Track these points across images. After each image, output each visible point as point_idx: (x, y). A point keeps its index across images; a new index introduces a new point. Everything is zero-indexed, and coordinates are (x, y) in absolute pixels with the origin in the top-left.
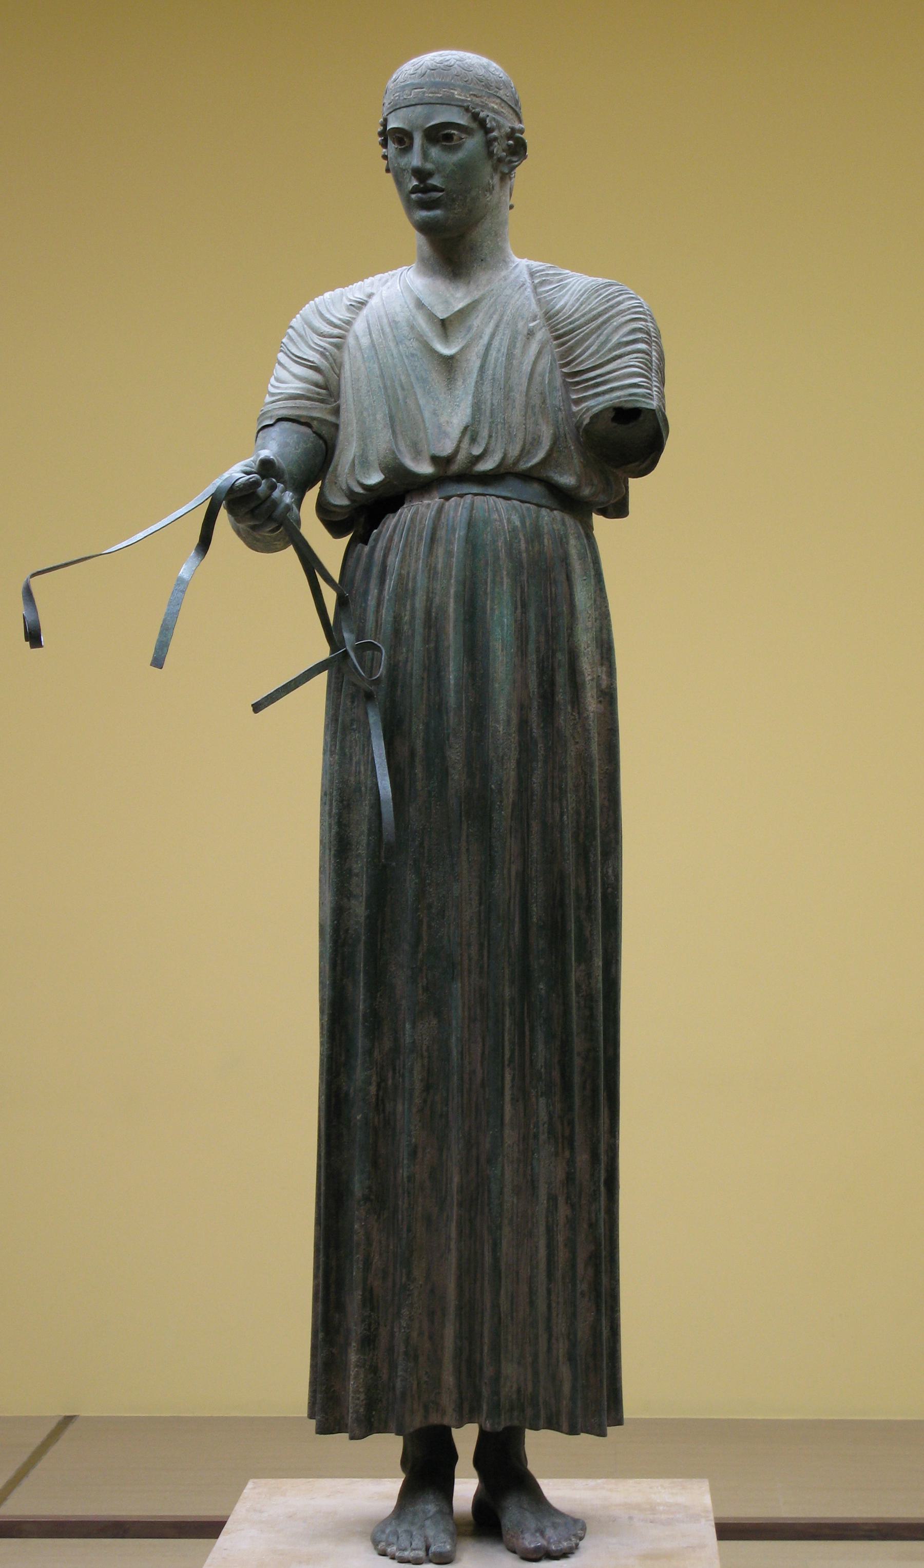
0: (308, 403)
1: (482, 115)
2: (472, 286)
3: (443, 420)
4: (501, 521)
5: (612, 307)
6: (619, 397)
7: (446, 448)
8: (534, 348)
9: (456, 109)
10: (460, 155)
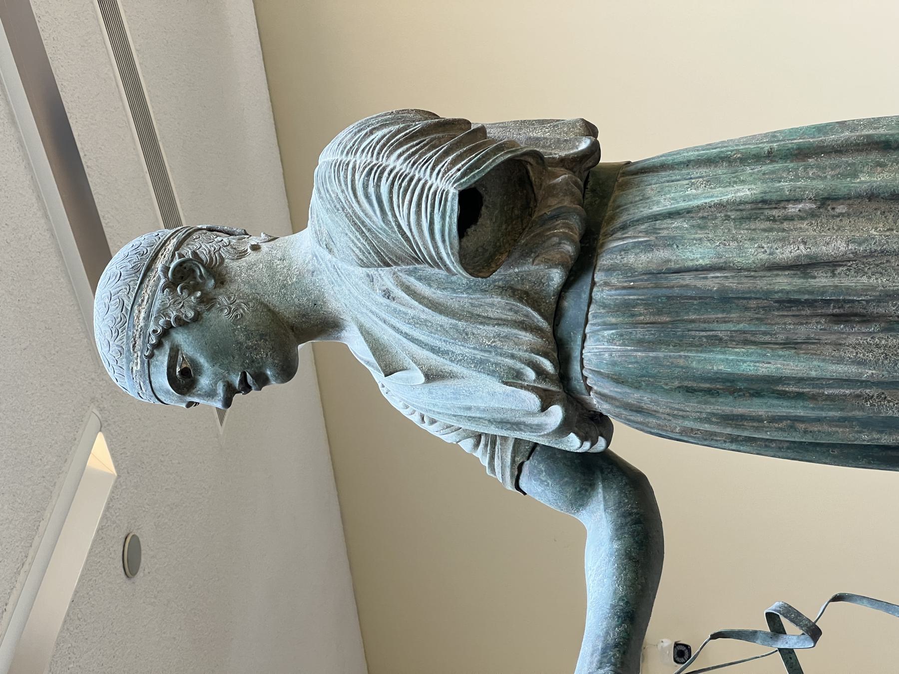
1: (154, 341)
2: (346, 323)
4: (611, 352)
6: (448, 254)
9: (153, 369)
10: (202, 360)
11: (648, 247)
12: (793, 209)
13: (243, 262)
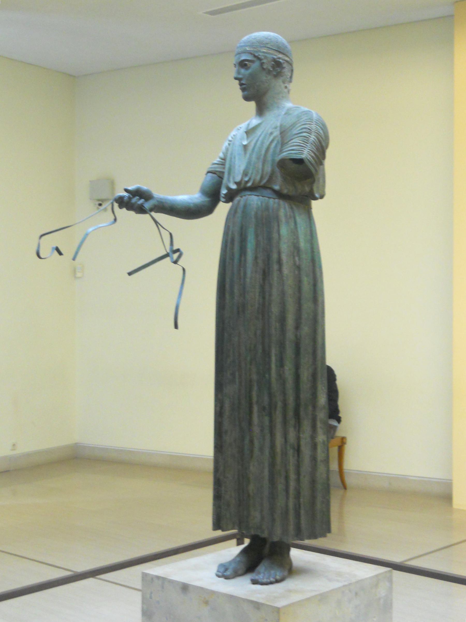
0: (216, 166)
1: (256, 54)
7: (238, 179)
8: (271, 138)
9: (247, 54)
11: (286, 216)
12: (297, 259)
13: (282, 84)
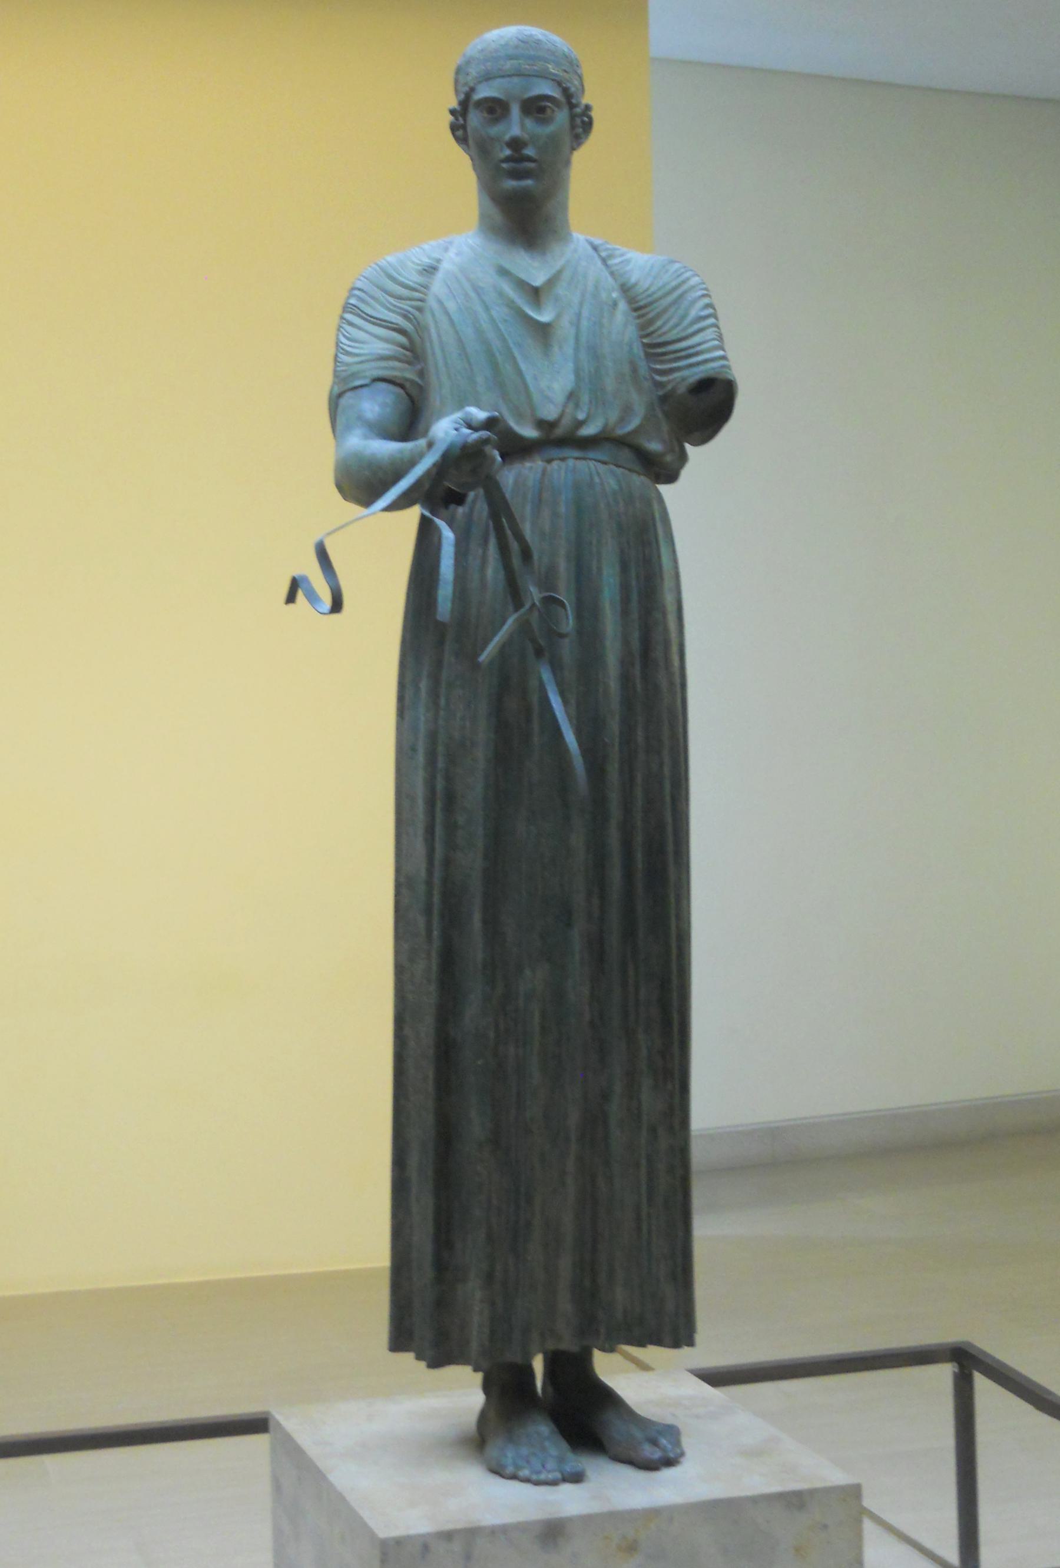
3: (543, 384)
4: (602, 484)
5: (684, 282)
7: (550, 413)
10: (550, 129)
